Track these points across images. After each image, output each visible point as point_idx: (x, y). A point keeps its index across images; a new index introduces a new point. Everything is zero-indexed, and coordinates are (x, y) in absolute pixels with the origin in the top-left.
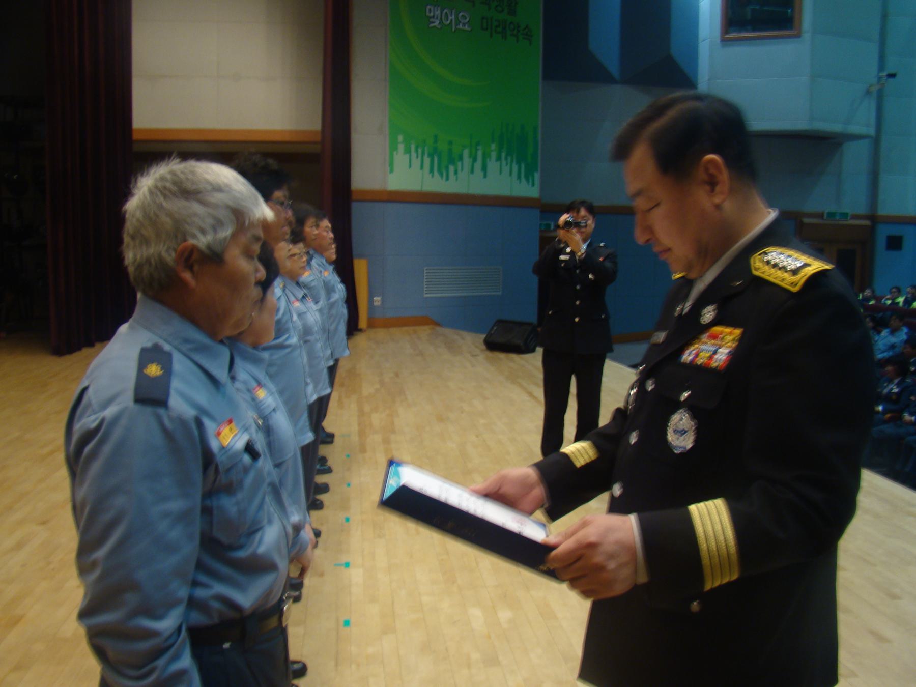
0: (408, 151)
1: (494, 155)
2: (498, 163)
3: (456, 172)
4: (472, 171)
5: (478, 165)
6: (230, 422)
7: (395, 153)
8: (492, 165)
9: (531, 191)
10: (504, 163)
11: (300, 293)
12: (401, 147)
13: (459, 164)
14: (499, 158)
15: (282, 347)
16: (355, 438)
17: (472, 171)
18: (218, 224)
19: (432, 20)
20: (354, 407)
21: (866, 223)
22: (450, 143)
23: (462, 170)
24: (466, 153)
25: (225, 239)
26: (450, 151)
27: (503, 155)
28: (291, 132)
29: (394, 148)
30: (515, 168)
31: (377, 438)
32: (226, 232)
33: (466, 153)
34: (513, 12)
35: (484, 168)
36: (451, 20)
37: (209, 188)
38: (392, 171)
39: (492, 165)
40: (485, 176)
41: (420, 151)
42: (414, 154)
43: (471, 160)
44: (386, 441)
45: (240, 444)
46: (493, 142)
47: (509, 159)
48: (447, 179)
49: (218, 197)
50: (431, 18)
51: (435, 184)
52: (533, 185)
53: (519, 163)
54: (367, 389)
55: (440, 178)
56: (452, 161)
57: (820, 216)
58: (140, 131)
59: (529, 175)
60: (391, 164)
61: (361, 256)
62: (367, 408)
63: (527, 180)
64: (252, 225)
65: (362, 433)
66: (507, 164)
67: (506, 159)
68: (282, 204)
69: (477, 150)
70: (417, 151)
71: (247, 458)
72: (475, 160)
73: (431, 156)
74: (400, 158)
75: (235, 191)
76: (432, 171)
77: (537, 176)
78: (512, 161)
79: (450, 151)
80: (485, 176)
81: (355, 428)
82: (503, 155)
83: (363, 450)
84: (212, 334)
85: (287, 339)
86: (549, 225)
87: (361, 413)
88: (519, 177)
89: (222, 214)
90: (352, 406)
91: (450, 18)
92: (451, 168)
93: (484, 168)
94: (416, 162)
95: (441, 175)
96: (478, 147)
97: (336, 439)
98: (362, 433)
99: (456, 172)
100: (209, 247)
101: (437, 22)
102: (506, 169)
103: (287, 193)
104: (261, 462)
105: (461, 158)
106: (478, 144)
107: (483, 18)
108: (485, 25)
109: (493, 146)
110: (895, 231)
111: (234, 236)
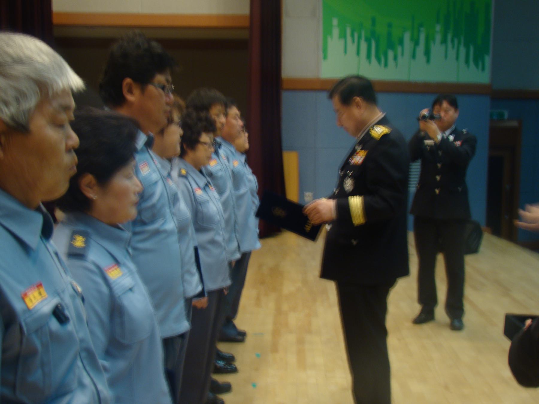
0: (343, 36)
1: (438, 38)
3: (395, 58)
4: (414, 56)
5: (421, 49)
6: (39, 286)
7: (329, 39)
8: (437, 49)
11: (202, 181)
12: (336, 32)
13: (399, 49)
14: (444, 41)
15: (157, 232)
16: (268, 338)
17: (414, 56)
18: (21, 96)
20: (272, 305)
22: (390, 25)
23: (402, 54)
25: (29, 110)
26: (389, 35)
27: (449, 37)
28: (218, 17)
29: (328, 32)
30: (462, 50)
31: (291, 338)
32: (31, 103)
35: (427, 53)
37: (9, 60)
38: (325, 57)
39: (437, 49)
40: (428, 61)
44: (301, 342)
45: (47, 308)
46: (438, 22)
48: (386, 65)
49: (18, 70)
52: (483, 69)
53: (467, 46)
54: (288, 288)
56: (391, 45)
58: (60, 14)
59: (478, 59)
60: (325, 51)
61: (292, 149)
62: (285, 307)
63: (477, 65)
64: (56, 95)
65: (276, 333)
67: (452, 41)
68: (163, 88)
69: (419, 31)
70: (352, 36)
71: (54, 324)
73: (368, 40)
75: (38, 62)
76: (369, 56)
77: (488, 60)
78: (459, 43)
79: (389, 35)
80: (428, 61)
81: (270, 327)
82: (449, 37)
83: (275, 349)
84: (27, 204)
85: (163, 224)
87: (279, 311)
88: (467, 61)
89: (25, 86)
90: (270, 304)
92: (391, 54)
93: (427, 53)
94: (352, 48)
95: (379, 60)
96: (422, 29)
97: (249, 339)
98: (276, 333)
99: (395, 58)
100: (13, 118)
102: (452, 53)
103: (170, 79)
104: (70, 327)
105: (401, 42)
106: (421, 25)
109: (438, 28)
111: (40, 106)
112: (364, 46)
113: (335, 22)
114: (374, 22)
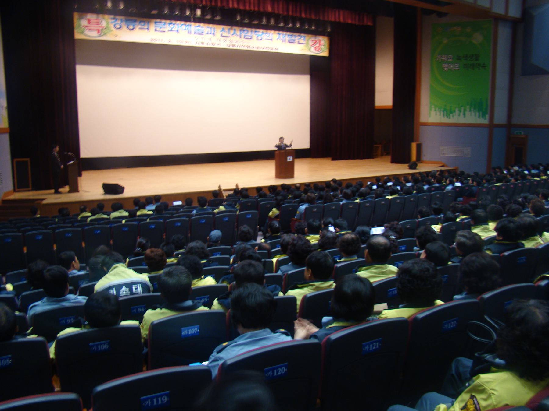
0: (435, 110)
1: (468, 110)
5: (462, 114)
8: (468, 113)
9: (486, 121)
12: (433, 109)
14: (470, 111)
22: (451, 107)
24: (457, 110)
29: (431, 110)
30: (477, 113)
34: (477, 60)
35: (464, 114)
39: (468, 113)
40: (465, 117)
51: (445, 120)
56: (451, 113)
59: (483, 116)
72: (460, 111)
74: (433, 113)
92: (451, 115)
93: (464, 114)
94: (438, 113)
105: (454, 111)
109: (468, 107)
113: (433, 106)
114: (445, 106)
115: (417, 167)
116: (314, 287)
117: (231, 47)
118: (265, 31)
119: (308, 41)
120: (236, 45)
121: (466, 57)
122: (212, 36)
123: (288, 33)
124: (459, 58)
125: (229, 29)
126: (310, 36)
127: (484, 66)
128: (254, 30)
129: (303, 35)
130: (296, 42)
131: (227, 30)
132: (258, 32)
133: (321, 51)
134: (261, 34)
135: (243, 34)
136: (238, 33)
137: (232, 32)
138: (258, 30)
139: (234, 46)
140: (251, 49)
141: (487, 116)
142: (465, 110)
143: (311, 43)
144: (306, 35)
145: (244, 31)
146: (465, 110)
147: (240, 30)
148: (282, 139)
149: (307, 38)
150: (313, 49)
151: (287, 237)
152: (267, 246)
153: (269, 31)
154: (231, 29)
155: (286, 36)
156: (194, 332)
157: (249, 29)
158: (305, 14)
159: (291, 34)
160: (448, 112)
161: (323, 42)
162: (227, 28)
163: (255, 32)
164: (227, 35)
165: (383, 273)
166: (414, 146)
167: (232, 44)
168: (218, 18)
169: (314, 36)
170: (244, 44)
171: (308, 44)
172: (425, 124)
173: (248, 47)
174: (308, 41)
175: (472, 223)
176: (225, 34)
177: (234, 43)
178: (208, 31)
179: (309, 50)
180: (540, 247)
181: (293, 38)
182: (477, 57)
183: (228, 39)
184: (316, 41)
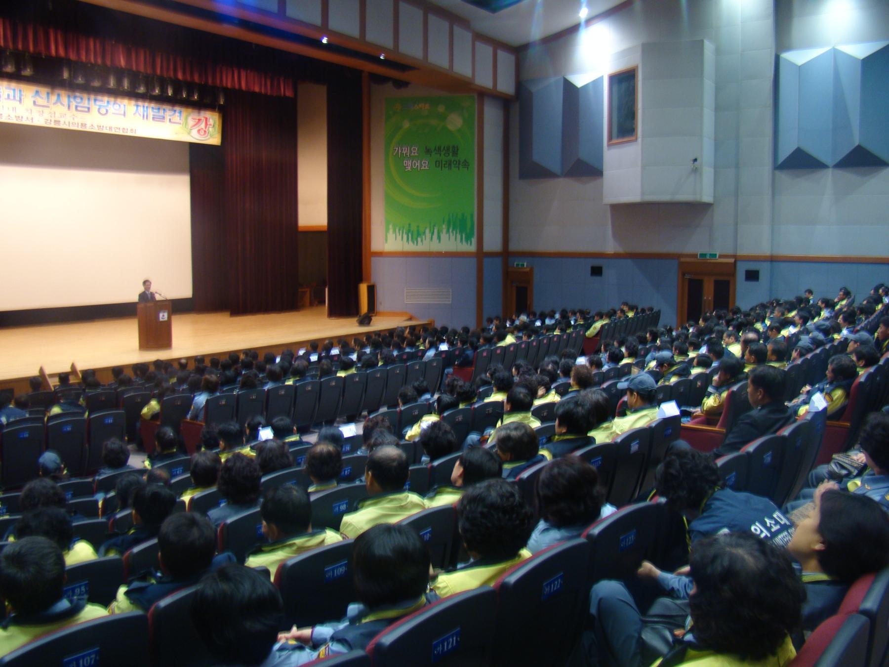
0: (394, 231)
1: (445, 231)
2: (448, 235)
3: (422, 241)
8: (444, 236)
10: (451, 234)
12: (391, 231)
13: (424, 237)
14: (448, 231)
19: (407, 167)
21: (732, 260)
24: (427, 231)
26: (418, 231)
27: (451, 230)
29: (387, 230)
30: (459, 236)
33: (427, 231)
35: (439, 238)
36: (418, 166)
39: (444, 236)
41: (401, 232)
42: (398, 234)
43: (430, 234)
47: (454, 232)
50: (405, 166)
51: (410, 247)
55: (413, 245)
56: (419, 235)
57: (695, 256)
59: (468, 239)
60: (386, 240)
66: (453, 235)
72: (433, 234)
74: (391, 235)
79: (418, 231)
86: (523, 265)
91: (417, 164)
92: (419, 239)
93: (439, 238)
94: (399, 237)
95: (414, 243)
99: (422, 241)
101: (410, 168)
105: (424, 233)
106: (434, 226)
107: (436, 162)
108: (438, 165)
109: (444, 226)
110: (752, 266)
112: (405, 236)
113: (391, 226)
114: (410, 225)
115: (372, 323)
116: (295, 548)
117: (53, 125)
118: (112, 100)
119: (186, 119)
120: (62, 122)
121: (438, 150)
122: (16, 104)
123: (153, 105)
124: (428, 151)
125: (48, 94)
126: (190, 110)
127: (466, 164)
128: (92, 97)
129: (177, 109)
130: (168, 118)
131: (44, 95)
132: (102, 101)
133: (209, 137)
134: (106, 104)
135: (73, 104)
136: (65, 100)
137: (54, 98)
138: (99, 98)
139: (57, 122)
140: (88, 129)
141: (474, 240)
142: (456, 233)
143: (191, 122)
144: (183, 110)
145: (75, 97)
146: (456, 233)
147: (69, 97)
148: (146, 283)
149: (184, 114)
150: (194, 132)
151: (203, 456)
152: (164, 474)
153: (119, 100)
154: (52, 93)
155: (150, 110)
156: (89, 663)
157: (85, 96)
158: (184, 73)
159: (158, 106)
160: (414, 235)
161: (211, 122)
162: (44, 91)
163: (95, 100)
164: (45, 103)
165: (403, 508)
166: (363, 288)
167: (53, 119)
168: (28, 72)
169: (196, 111)
170: (76, 121)
171: (186, 123)
172: (380, 254)
173: (84, 125)
174: (186, 119)
175: (507, 407)
176: (40, 101)
177: (57, 119)
178: (8, 95)
179: (189, 133)
180: (619, 440)
181: (161, 113)
182: (455, 151)
183: (46, 110)
184: (199, 120)
